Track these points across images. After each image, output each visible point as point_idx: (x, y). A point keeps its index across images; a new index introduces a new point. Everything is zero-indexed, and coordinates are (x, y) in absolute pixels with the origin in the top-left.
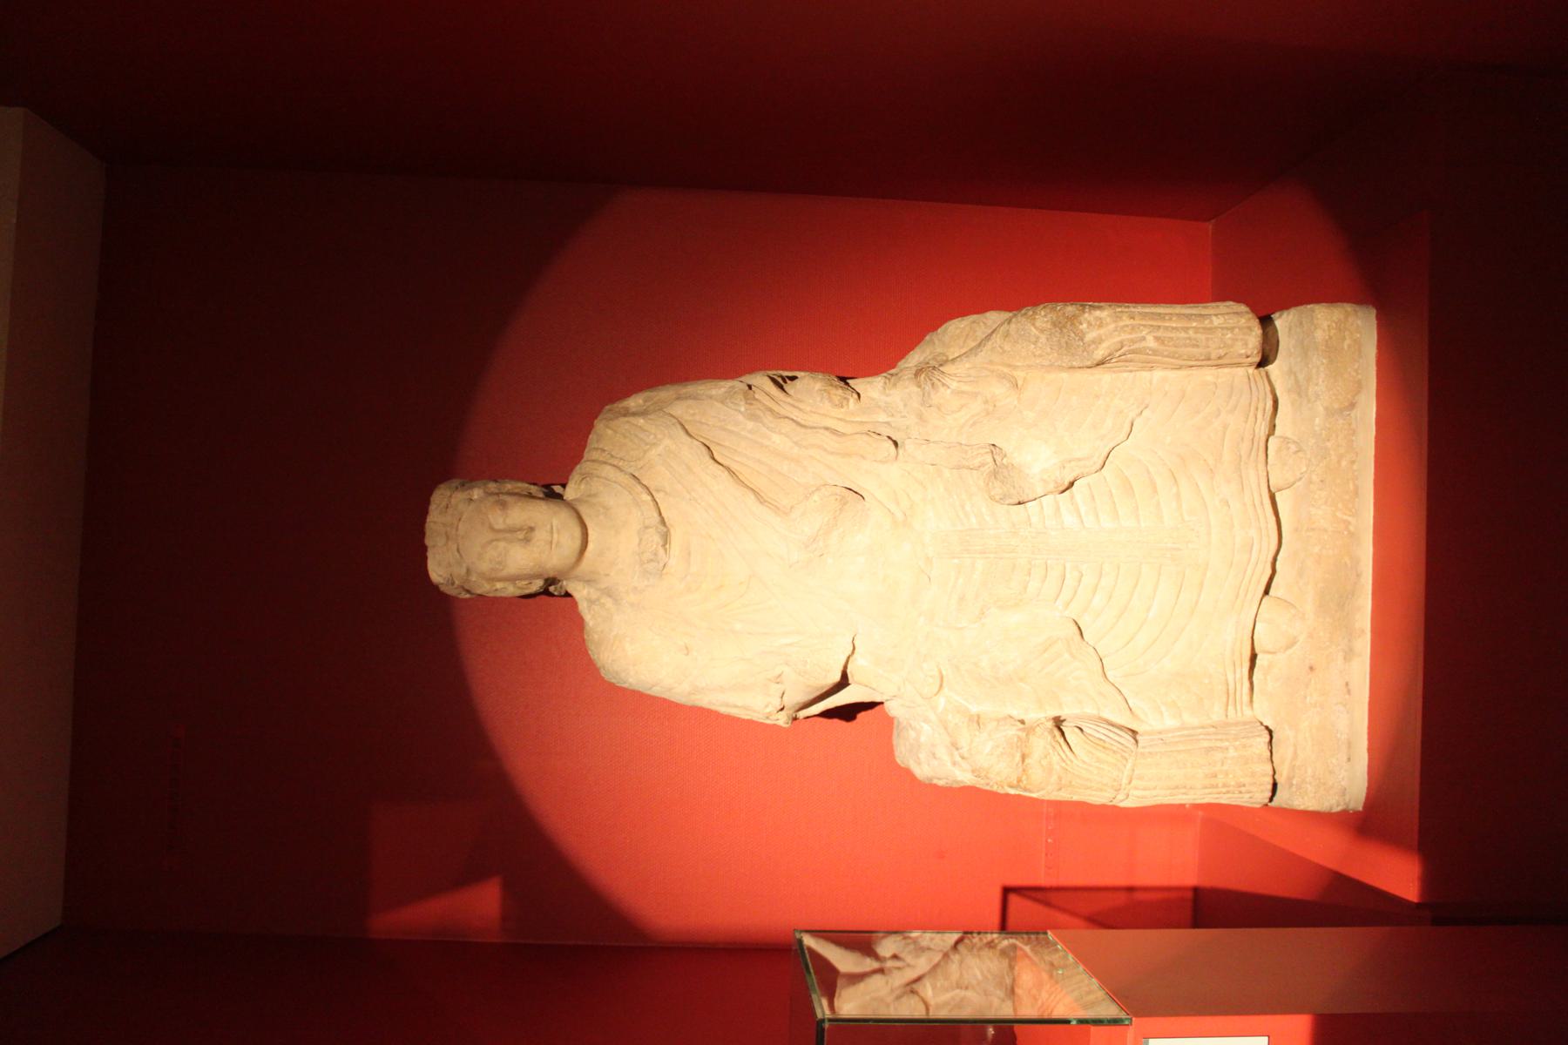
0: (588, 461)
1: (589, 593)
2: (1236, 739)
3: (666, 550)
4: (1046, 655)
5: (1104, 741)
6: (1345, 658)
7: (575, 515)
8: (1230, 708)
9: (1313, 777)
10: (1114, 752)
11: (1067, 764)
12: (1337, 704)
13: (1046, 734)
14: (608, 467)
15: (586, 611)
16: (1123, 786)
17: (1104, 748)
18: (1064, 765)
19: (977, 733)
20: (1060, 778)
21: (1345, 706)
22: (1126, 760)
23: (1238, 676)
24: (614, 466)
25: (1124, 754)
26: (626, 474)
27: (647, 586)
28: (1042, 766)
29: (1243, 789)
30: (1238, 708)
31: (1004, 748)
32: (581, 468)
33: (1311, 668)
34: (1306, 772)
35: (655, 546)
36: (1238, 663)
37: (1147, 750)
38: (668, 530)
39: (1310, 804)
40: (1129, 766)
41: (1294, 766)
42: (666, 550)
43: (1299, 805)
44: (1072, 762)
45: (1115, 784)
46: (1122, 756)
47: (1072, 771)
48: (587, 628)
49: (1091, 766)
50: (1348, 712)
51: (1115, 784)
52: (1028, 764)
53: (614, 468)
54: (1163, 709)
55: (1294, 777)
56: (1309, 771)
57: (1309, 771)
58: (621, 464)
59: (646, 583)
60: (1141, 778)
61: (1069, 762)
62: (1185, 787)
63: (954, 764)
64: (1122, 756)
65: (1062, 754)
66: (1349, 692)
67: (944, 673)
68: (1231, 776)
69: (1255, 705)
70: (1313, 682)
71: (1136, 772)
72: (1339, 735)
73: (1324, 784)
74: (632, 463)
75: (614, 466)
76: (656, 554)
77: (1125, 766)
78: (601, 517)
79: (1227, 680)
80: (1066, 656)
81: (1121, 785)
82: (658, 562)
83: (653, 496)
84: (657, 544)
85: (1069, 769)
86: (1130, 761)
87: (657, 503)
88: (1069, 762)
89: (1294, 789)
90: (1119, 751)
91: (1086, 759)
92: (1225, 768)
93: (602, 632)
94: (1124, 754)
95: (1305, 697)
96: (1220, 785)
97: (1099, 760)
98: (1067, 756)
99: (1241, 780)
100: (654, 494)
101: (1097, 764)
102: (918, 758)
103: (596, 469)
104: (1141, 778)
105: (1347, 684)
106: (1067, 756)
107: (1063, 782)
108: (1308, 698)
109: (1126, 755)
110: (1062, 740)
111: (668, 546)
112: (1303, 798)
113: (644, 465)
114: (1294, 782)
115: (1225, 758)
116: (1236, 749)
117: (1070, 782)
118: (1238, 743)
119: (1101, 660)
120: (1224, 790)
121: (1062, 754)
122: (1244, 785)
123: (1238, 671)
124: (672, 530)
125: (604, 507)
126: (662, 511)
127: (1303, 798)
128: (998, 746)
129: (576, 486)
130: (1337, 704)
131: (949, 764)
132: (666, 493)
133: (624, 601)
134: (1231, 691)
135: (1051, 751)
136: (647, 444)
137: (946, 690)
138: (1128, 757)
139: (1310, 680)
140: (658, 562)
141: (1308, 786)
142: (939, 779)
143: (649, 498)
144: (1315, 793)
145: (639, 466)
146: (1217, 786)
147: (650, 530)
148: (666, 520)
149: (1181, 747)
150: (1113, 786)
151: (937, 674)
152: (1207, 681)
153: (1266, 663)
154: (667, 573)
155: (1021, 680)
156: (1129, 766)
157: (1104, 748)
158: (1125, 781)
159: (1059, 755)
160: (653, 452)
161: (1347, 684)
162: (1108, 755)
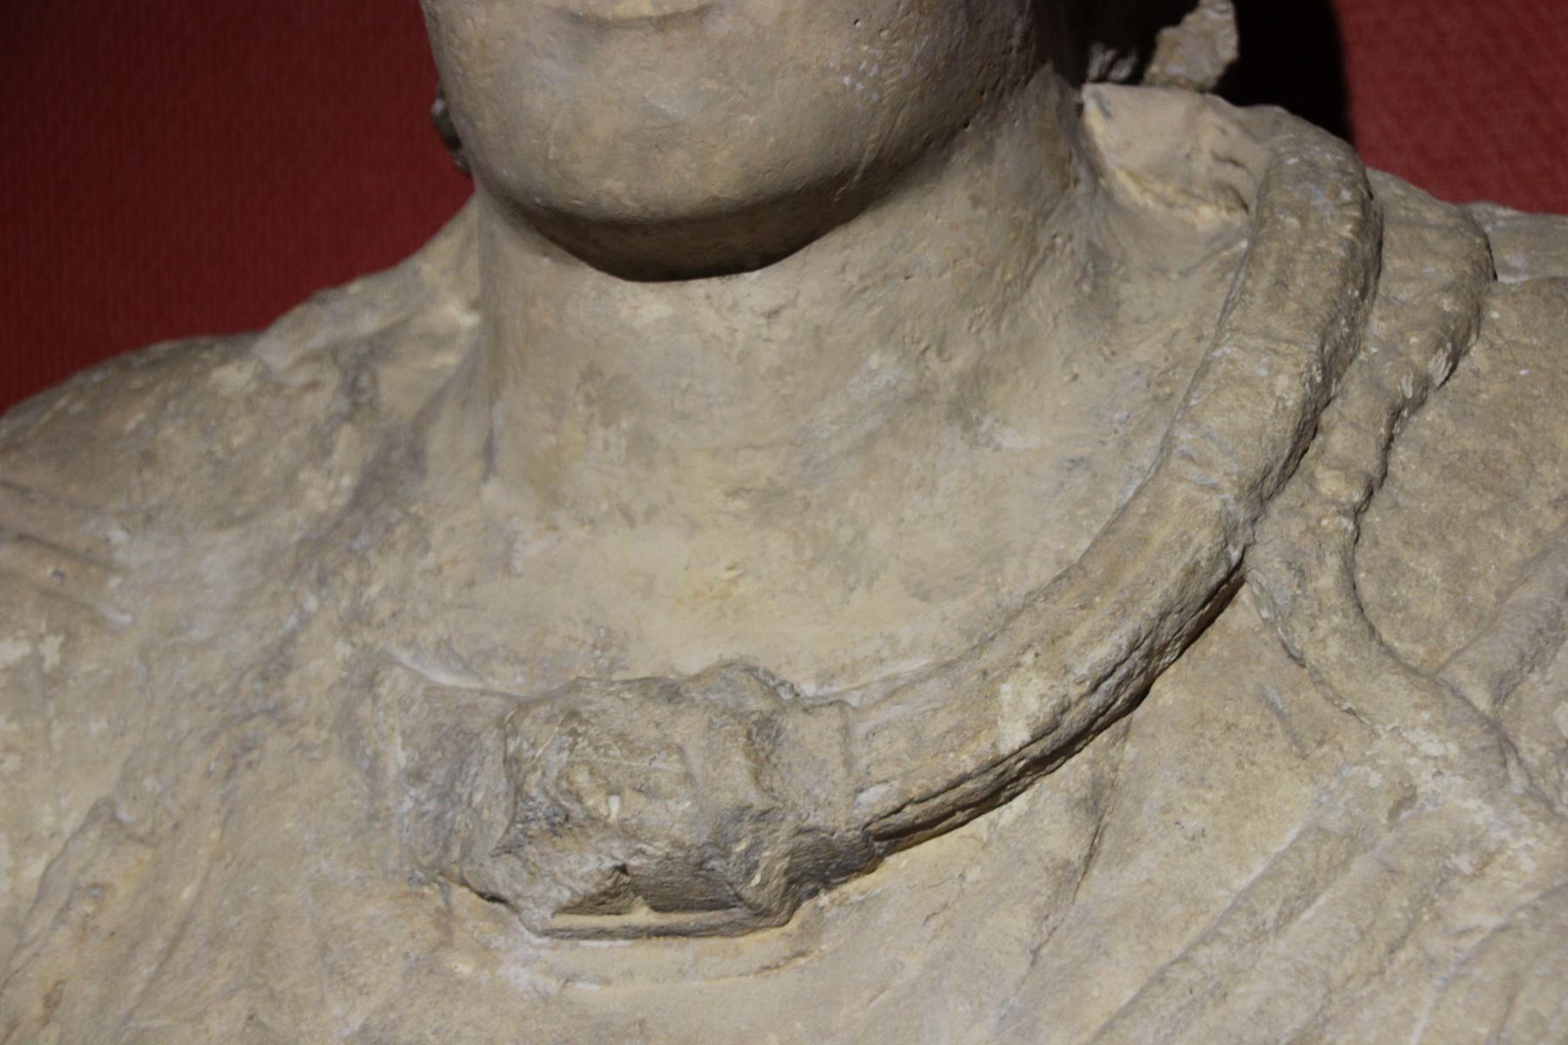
0: (1372, 227)
1: (439, 341)
3: (606, 899)
7: (867, 142)
14: (1289, 389)
15: (318, 341)
24: (1308, 429)
26: (1228, 532)
27: (373, 773)
32: (1312, 170)
35: (614, 808)
38: (761, 916)
42: (606, 899)
48: (209, 350)
53: (1283, 430)
58: (1330, 483)
59: (398, 757)
74: (1326, 580)
75: (1308, 429)
76: (561, 824)
78: (883, 367)
82: (509, 849)
83: (1043, 764)
84: (628, 832)
87: (989, 801)
93: (148, 458)
100: (1074, 772)
103: (1281, 284)
111: (642, 916)
113: (1318, 680)
124: (763, 944)
125: (977, 382)
126: (929, 850)
129: (1202, 165)
132: (1069, 876)
133: (312, 603)
136: (1503, 687)
140: (509, 849)
143: (1014, 735)
145: (1301, 639)
147: (738, 766)
148: (854, 888)
154: (445, 919)
160: (1432, 746)
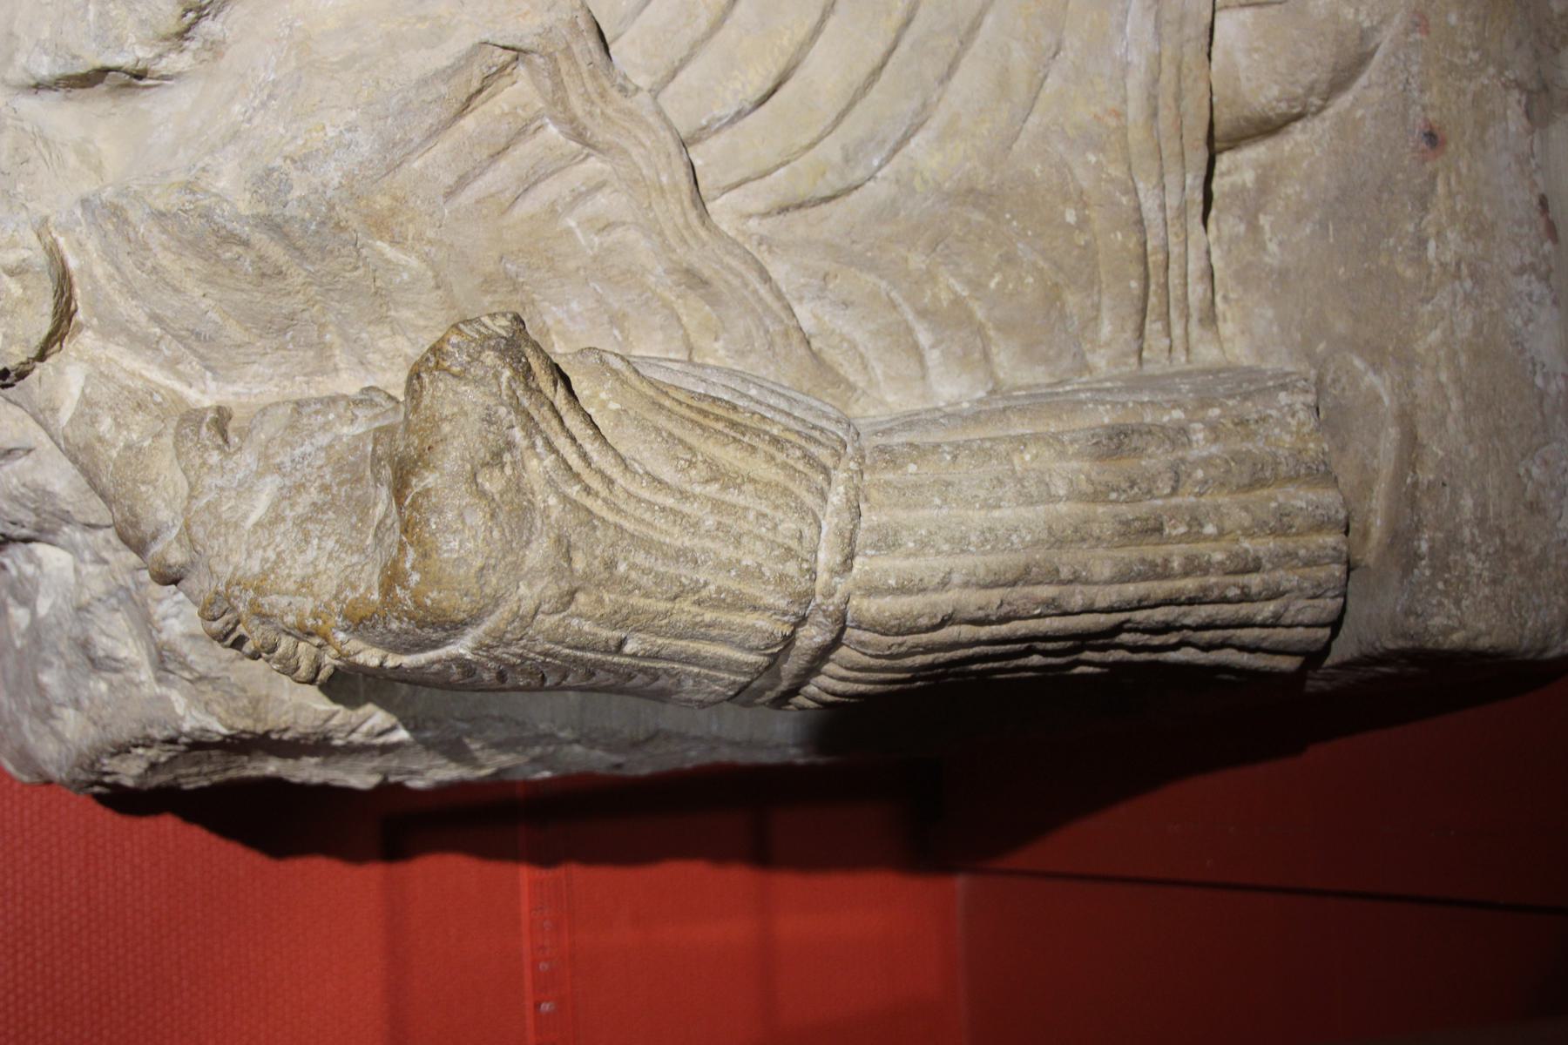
2: (1204, 404)
4: (469, 123)
5: (735, 408)
6: (1528, 114)
8: (1153, 327)
9: (1481, 522)
10: (775, 441)
11: (587, 490)
12: (1521, 270)
13: (489, 357)
16: (823, 577)
17: (733, 424)
18: (574, 491)
19: (214, 458)
20: (565, 548)
21: (1545, 278)
22: (825, 470)
23: (1172, 201)
25: (813, 449)
28: (483, 494)
29: (1255, 581)
30: (1177, 331)
31: (325, 488)
33: (1433, 138)
34: (1455, 506)
36: (1170, 148)
37: (897, 439)
39: (1482, 626)
40: (836, 497)
41: (1415, 485)
43: (1447, 631)
44: (610, 482)
45: (791, 568)
46: (807, 457)
47: (611, 517)
49: (684, 495)
50: (1555, 302)
51: (791, 568)
52: (426, 493)
54: (924, 338)
55: (1417, 528)
56: (1467, 502)
57: (1467, 502)
60: (887, 541)
61: (596, 484)
62: (1053, 577)
63: (164, 660)
64: (807, 457)
65: (562, 443)
66: (1552, 231)
67: (73, 263)
68: (1210, 529)
69: (1227, 328)
70: (1441, 188)
71: (870, 518)
72: (1539, 381)
73: (1519, 550)
77: (823, 496)
79: (1138, 208)
80: (552, 130)
81: (812, 572)
85: (596, 506)
86: (840, 476)
88: (596, 484)
89: (1424, 570)
90: (793, 437)
91: (667, 473)
92: (1185, 499)
94: (813, 449)
95: (1422, 243)
96: (1176, 564)
97: (716, 474)
98: (584, 456)
99: (1246, 544)
101: (713, 489)
102: (40, 689)
104: (887, 541)
105: (1543, 203)
106: (584, 456)
107: (579, 564)
108: (1432, 245)
109: (824, 455)
110: (560, 399)
112: (1457, 603)
114: (1424, 547)
115: (1183, 461)
116: (1214, 429)
117: (610, 565)
118: (1215, 412)
119: (684, 144)
120: (1190, 585)
121: (562, 443)
122: (1257, 568)
123: (1172, 180)
127: (1457, 603)
128: (300, 487)
130: (1521, 270)
131: (145, 674)
134: (1155, 259)
135: (518, 434)
137: (85, 342)
138: (829, 463)
139: (1434, 177)
141: (1471, 557)
142: (123, 750)
144: (1494, 582)
146: (1161, 572)
149: (1020, 428)
150: (782, 578)
151: (40, 259)
152: (1071, 217)
153: (1248, 177)
155: (379, 225)
156: (836, 497)
157: (733, 424)
158: (827, 557)
159: (552, 449)
161: (1543, 203)
162: (754, 449)
